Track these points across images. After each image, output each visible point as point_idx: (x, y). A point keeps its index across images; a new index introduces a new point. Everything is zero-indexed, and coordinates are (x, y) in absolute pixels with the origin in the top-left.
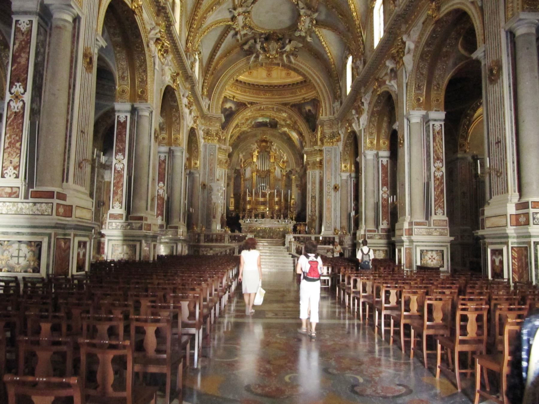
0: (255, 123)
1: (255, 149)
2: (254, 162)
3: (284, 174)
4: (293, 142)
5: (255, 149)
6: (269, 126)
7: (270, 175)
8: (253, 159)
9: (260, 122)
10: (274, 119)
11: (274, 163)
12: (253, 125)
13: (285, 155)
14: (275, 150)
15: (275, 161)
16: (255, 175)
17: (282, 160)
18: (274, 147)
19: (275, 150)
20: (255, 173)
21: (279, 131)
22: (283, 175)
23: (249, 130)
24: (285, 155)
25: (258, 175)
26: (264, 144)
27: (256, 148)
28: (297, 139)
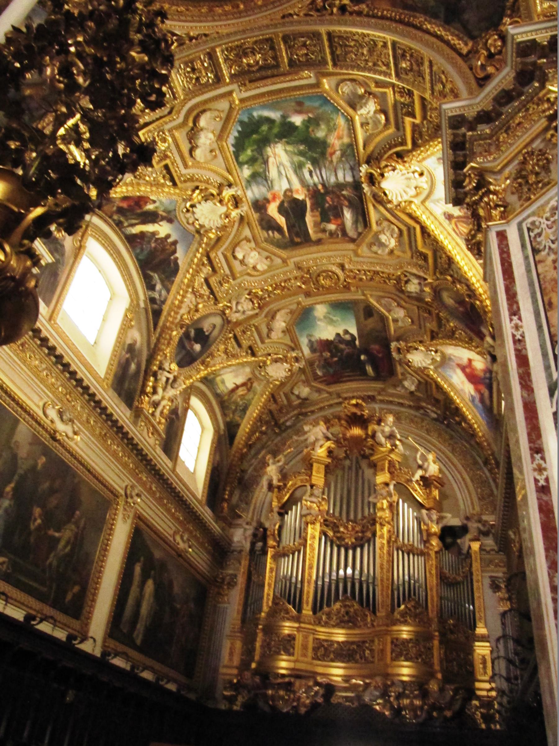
0: (313, 349)
1: (317, 440)
2: (312, 486)
3: (435, 528)
4: (457, 411)
5: (317, 440)
6: (369, 369)
7: (374, 534)
8: (310, 476)
9: (326, 345)
10: (369, 311)
11: (387, 484)
12: (311, 363)
13: (431, 457)
14: (391, 437)
15: (392, 479)
16: (317, 534)
17: (420, 473)
18: (387, 429)
19: (391, 437)
20: (318, 526)
21: (406, 384)
22: (430, 535)
23: (304, 391)
24: (431, 457)
25: (330, 534)
26: (357, 431)
27: (320, 436)
28: (473, 400)
